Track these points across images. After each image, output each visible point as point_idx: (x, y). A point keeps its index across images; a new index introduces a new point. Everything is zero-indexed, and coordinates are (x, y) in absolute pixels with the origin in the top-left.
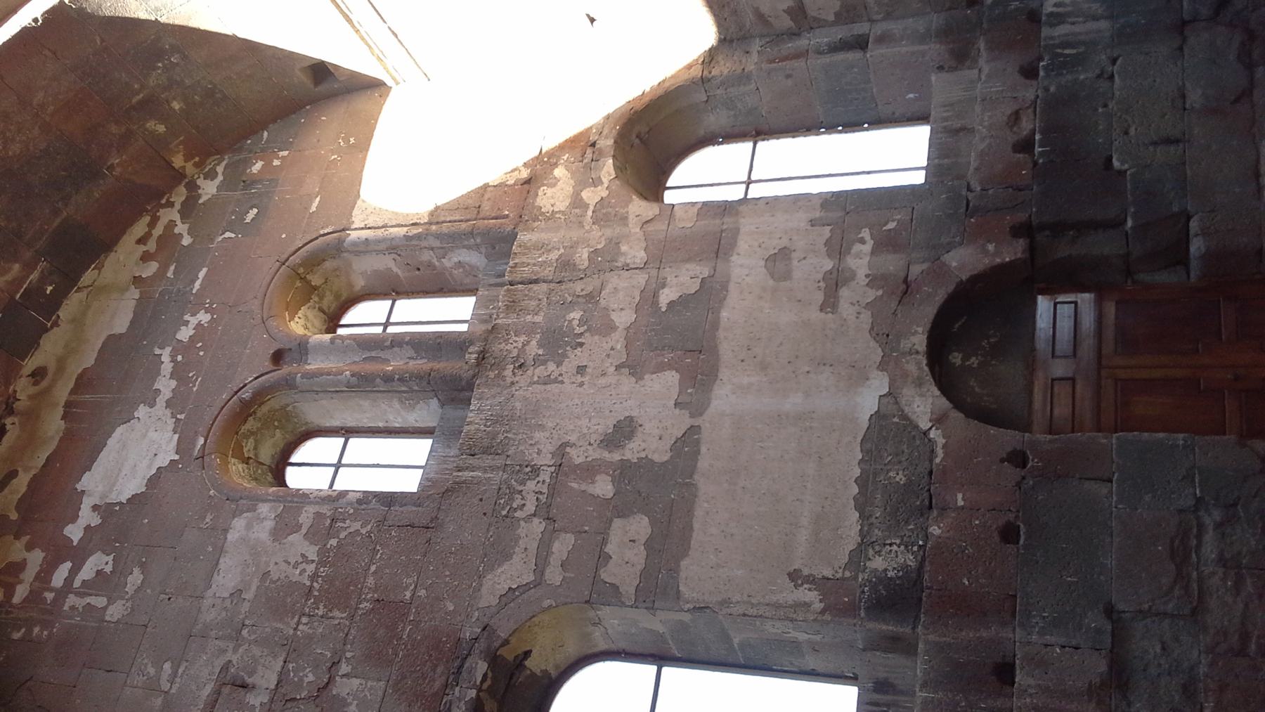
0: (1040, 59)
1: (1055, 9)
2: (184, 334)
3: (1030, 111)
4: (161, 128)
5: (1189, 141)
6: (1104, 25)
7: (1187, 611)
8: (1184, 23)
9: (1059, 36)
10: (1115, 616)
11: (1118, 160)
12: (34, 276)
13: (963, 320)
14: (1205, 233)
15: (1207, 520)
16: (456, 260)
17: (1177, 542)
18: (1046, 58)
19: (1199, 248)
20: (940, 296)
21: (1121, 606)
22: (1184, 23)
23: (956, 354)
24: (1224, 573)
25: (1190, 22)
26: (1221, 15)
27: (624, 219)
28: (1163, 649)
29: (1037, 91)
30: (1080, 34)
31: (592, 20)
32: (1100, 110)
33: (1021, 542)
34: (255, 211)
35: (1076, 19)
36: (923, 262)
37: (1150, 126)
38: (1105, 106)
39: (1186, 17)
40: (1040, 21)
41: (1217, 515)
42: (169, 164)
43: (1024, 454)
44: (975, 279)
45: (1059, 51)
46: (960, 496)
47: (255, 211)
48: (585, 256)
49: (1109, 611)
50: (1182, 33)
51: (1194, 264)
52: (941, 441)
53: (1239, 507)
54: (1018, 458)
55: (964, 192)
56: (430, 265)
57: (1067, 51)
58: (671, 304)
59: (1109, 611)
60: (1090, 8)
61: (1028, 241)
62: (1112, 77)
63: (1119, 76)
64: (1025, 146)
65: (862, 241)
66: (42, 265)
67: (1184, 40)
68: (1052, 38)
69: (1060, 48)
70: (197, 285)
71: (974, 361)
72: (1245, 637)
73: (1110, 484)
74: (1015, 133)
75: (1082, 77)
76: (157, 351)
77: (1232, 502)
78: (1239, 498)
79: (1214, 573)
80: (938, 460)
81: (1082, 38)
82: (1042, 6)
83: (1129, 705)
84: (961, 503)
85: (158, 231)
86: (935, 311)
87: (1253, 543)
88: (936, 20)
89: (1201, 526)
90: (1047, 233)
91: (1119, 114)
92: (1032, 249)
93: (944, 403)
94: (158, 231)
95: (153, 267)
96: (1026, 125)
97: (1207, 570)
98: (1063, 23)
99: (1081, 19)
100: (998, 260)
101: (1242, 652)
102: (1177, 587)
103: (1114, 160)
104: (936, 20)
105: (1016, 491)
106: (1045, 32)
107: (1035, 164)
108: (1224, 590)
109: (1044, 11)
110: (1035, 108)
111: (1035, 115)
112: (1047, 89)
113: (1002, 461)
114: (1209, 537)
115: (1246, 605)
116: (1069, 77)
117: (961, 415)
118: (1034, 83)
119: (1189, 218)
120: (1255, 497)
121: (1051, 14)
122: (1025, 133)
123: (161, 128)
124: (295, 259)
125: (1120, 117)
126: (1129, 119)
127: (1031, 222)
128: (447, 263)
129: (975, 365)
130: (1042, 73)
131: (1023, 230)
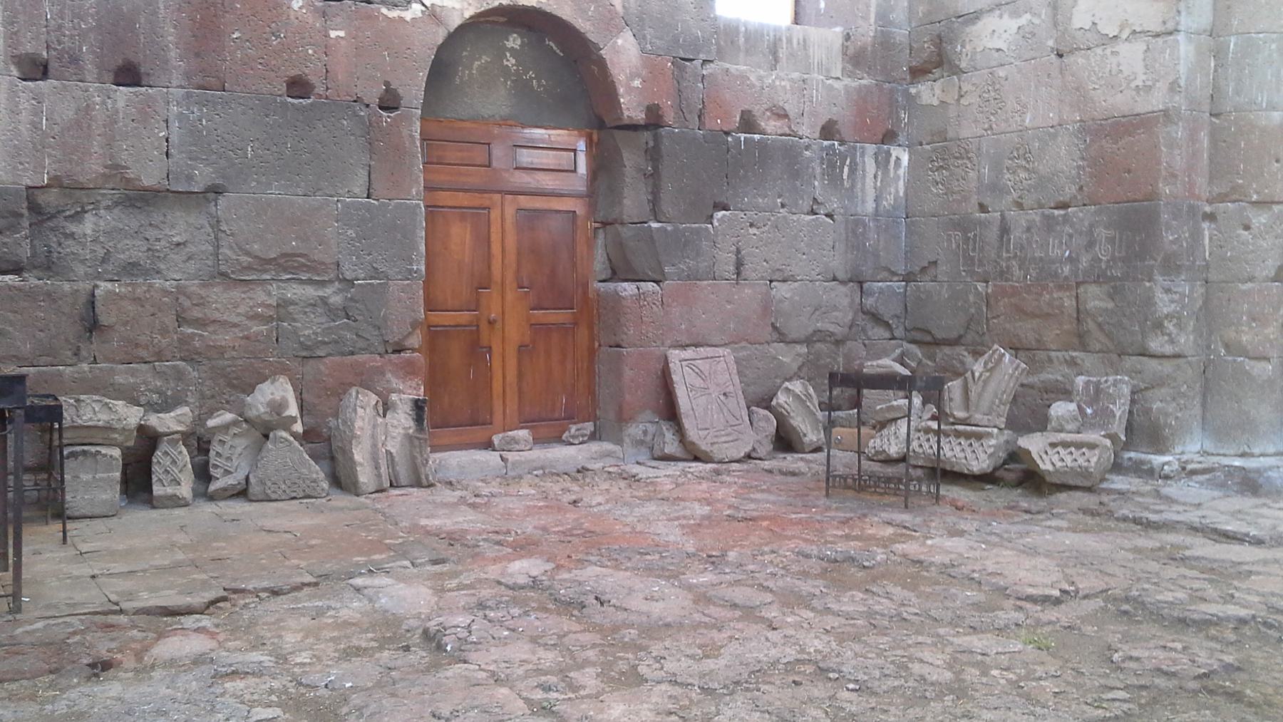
0: (842, 142)
1: (893, 159)
3: (787, 130)
5: (737, 284)
6: (870, 206)
7: (223, 268)
8: (861, 283)
9: (864, 162)
10: (211, 196)
11: (724, 215)
13: (558, 51)
14: (640, 296)
15: (328, 291)
17: (302, 260)
18: (842, 148)
19: (625, 290)
20: (581, 24)
21: (222, 201)
22: (861, 283)
23: (519, 42)
24: (270, 305)
25: (862, 288)
26: (864, 317)
28: (178, 244)
29: (807, 137)
30: (863, 184)
32: (779, 200)
33: (290, 100)
35: (879, 180)
36: (624, 7)
37: (757, 248)
38: (783, 206)
39: (866, 286)
40: (883, 143)
41: (336, 300)
43: (396, 108)
44: (602, 63)
45: (848, 162)
46: (342, 34)
49: (217, 190)
50: (851, 280)
51: (611, 285)
52: (408, 15)
53: (345, 320)
54: (390, 102)
55: (702, 56)
57: (846, 169)
59: (217, 190)
60: (890, 194)
61: (642, 122)
62: (813, 212)
63: (813, 220)
64: (748, 123)
67: (843, 283)
68: (863, 155)
69: (850, 163)
71: (510, 62)
72: (201, 323)
73: (365, 196)
74: (764, 113)
75: (816, 183)
77: (350, 314)
78: (355, 321)
79: (269, 294)
80: (384, 11)
81: (859, 186)
82: (899, 145)
83: (108, 208)
84: (333, 34)
86: (564, 17)
87: (306, 333)
88: (901, 34)
89: (322, 284)
90: (651, 144)
91: (772, 218)
92: (634, 127)
93: (456, 22)
96: (771, 126)
97: (273, 288)
98: (878, 167)
99: (879, 184)
100: (621, 90)
101: (181, 320)
102: (250, 259)
103: (724, 212)
104: (901, 34)
105: (352, 97)
106: (871, 148)
107: (727, 133)
108: (251, 304)
109: (892, 148)
110: (790, 135)
111: (781, 135)
112: (807, 148)
113: (387, 84)
114: (311, 292)
115: (235, 325)
116: (818, 170)
117: (440, 41)
118: (817, 135)
119: (657, 282)
120: (357, 335)
121: (889, 154)
122: (763, 124)
125: (769, 220)
126: (766, 228)
127: (663, 127)
129: (505, 63)
130: (826, 143)
131: (654, 121)
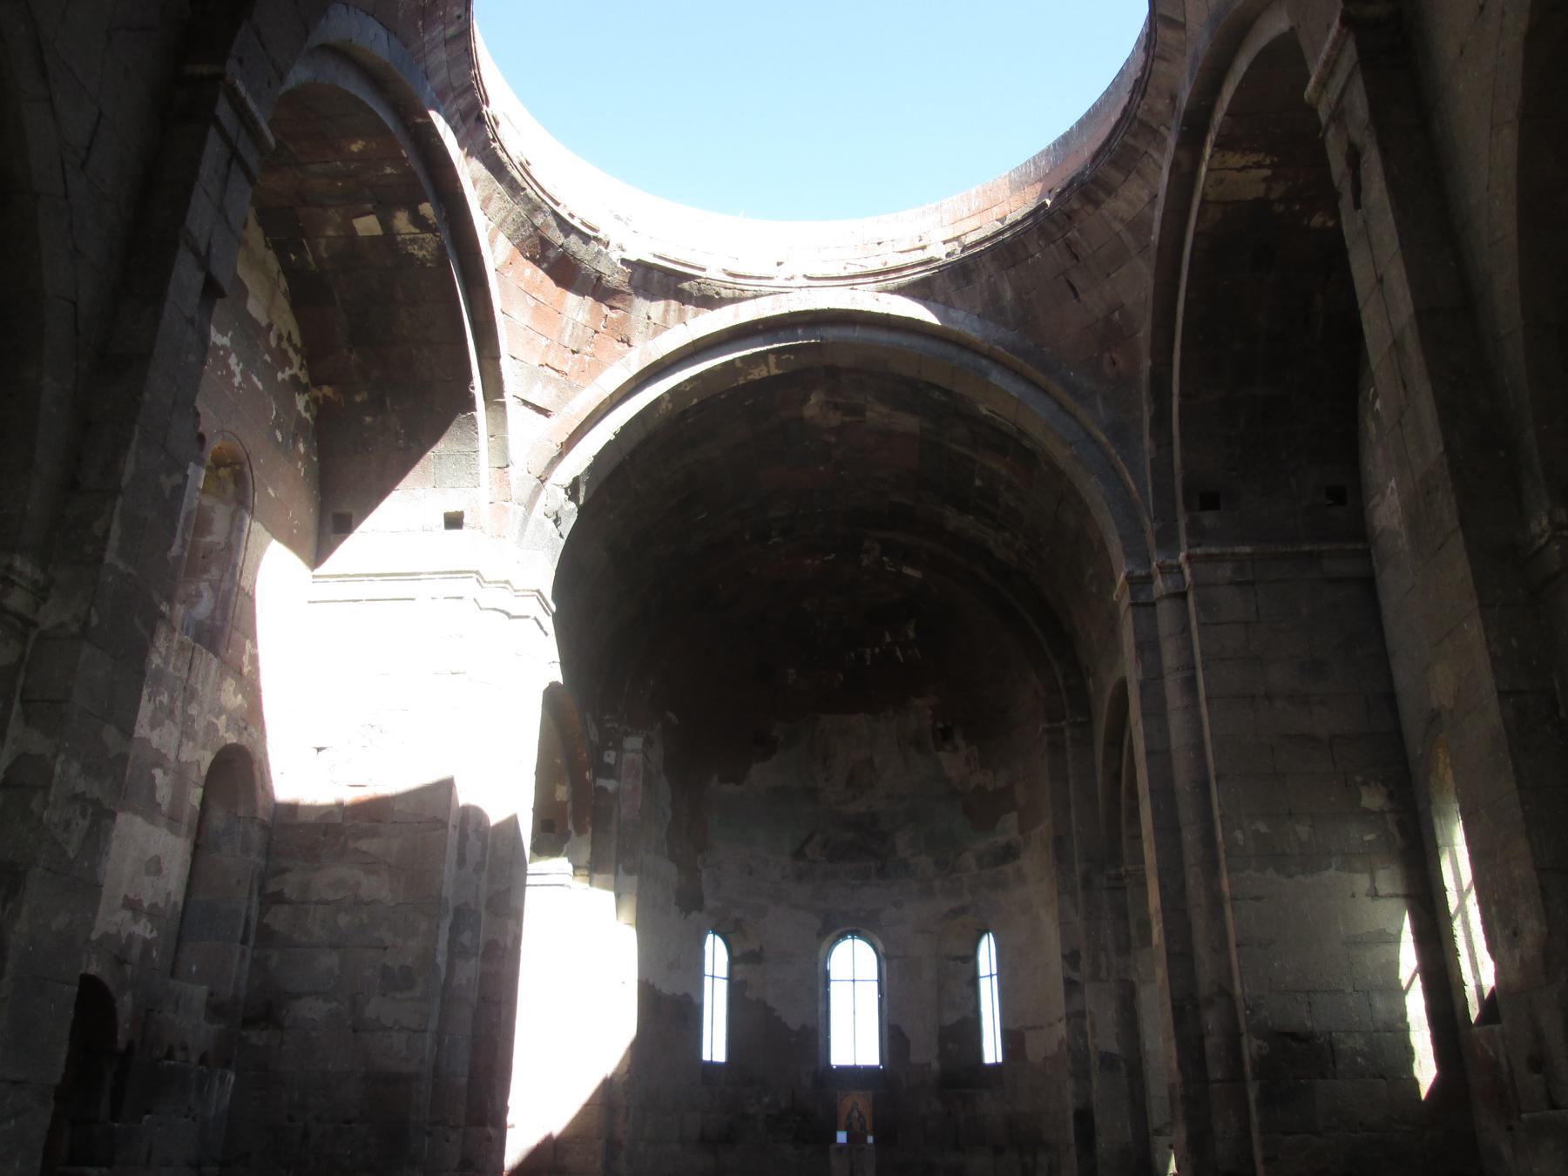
2: (233, 360)
4: (358, 399)
12: (310, 258)
16: (205, 594)
27: (204, 747)
31: (319, 750)
34: (280, 440)
42: (330, 384)
47: (280, 440)
48: (193, 713)
56: (206, 570)
58: (153, 778)
65: (151, 931)
66: (313, 266)
70: (255, 379)
76: (230, 334)
85: (291, 353)
94: (291, 353)
95: (273, 343)
123: (358, 399)
124: (247, 469)
128: (204, 586)
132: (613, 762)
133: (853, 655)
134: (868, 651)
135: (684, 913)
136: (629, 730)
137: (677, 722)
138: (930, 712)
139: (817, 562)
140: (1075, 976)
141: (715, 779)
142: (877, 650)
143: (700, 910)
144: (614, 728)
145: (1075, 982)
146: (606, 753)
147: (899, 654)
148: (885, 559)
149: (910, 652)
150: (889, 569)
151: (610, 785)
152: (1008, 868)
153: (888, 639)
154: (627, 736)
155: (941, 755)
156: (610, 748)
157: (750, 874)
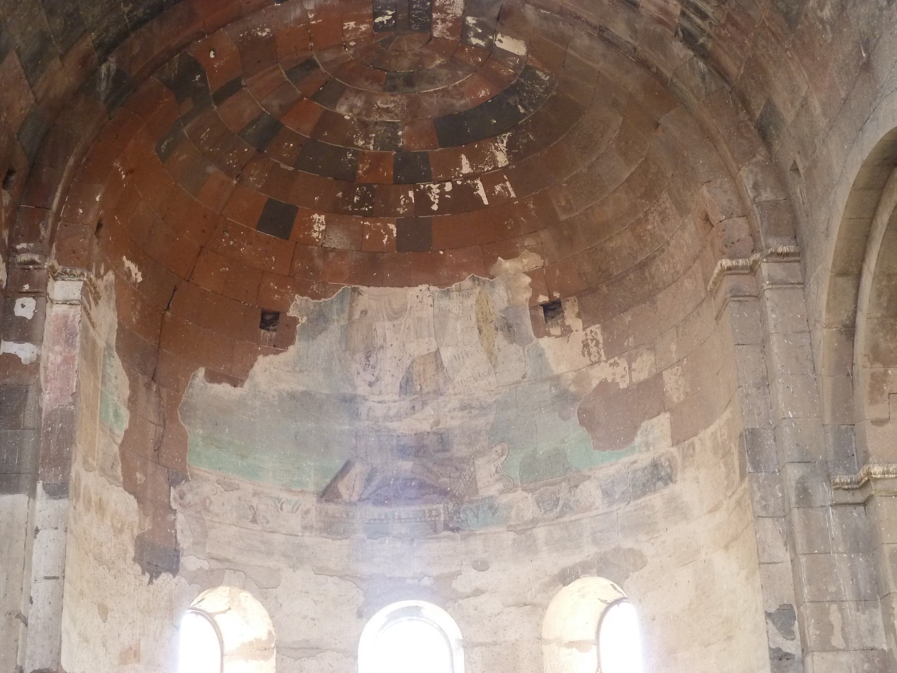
132: (29, 316)
133: (411, 194)
134: (435, 188)
135: (147, 576)
136: (59, 268)
137: (140, 279)
138: (528, 280)
139: (363, 27)
140: (791, 647)
141: (201, 372)
142: (448, 187)
143: (174, 568)
144: (33, 262)
145: (788, 656)
146: (19, 302)
147: (481, 192)
148: (470, 20)
149: (498, 188)
150: (475, 41)
151: (24, 351)
152: (656, 500)
153: (466, 169)
154: (55, 279)
155: (544, 342)
156: (27, 294)
157: (254, 521)
